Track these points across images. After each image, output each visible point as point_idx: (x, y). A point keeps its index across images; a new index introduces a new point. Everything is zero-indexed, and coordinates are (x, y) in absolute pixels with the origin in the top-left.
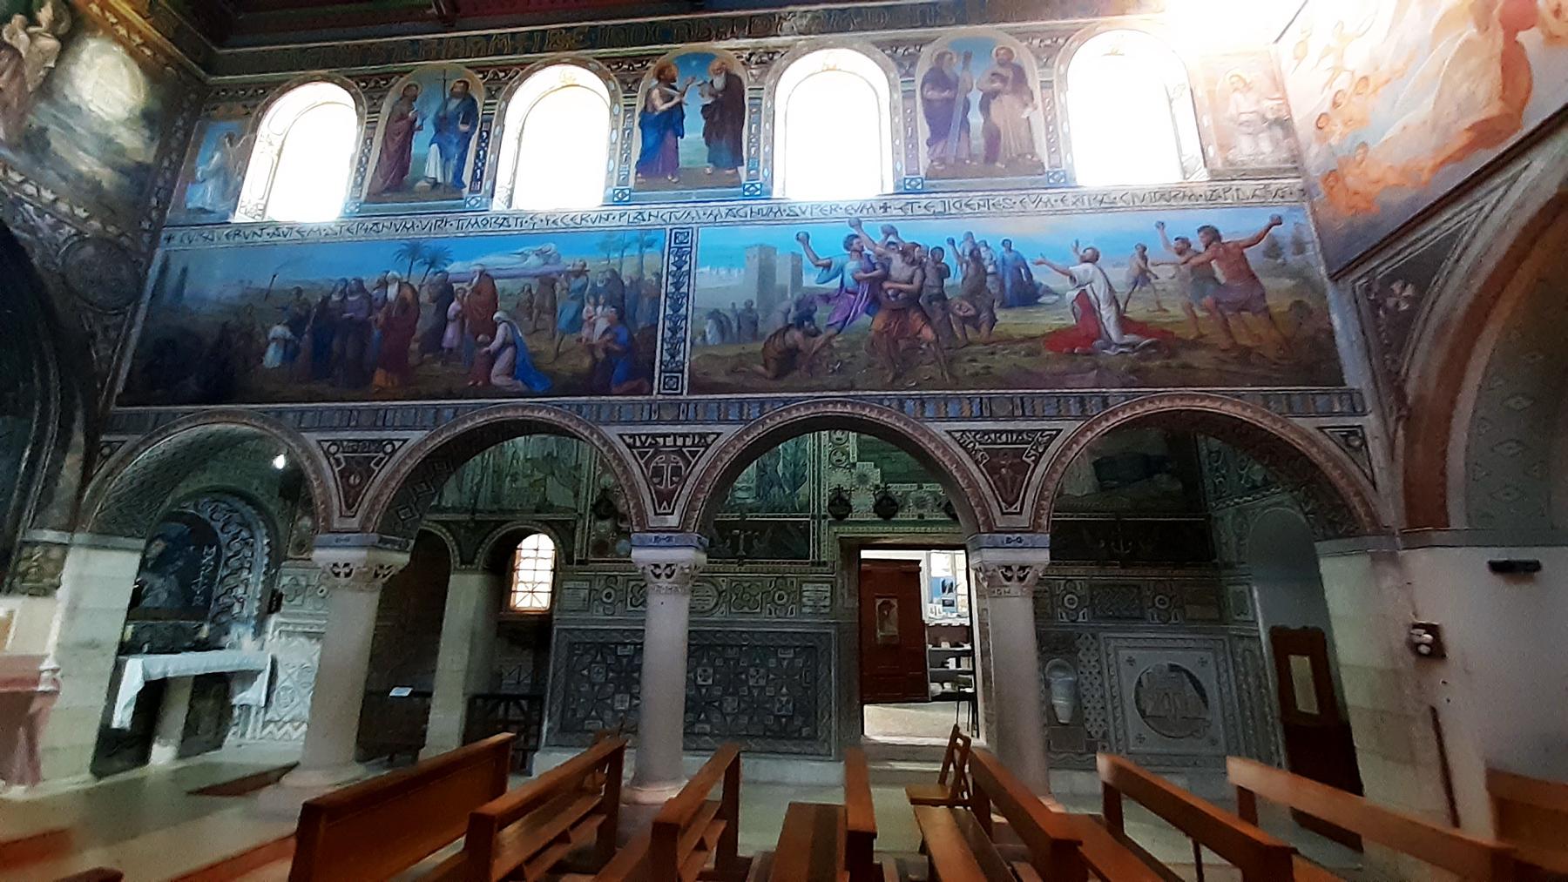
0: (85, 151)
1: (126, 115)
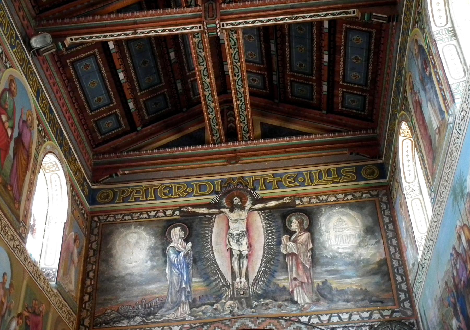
0: (349, 277)
1: (358, 241)
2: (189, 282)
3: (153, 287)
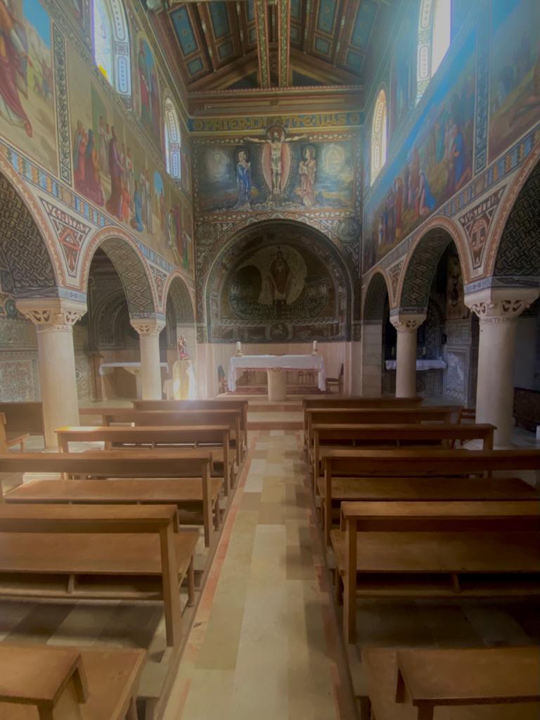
0: (333, 191)
2: (249, 189)
3: (230, 191)
